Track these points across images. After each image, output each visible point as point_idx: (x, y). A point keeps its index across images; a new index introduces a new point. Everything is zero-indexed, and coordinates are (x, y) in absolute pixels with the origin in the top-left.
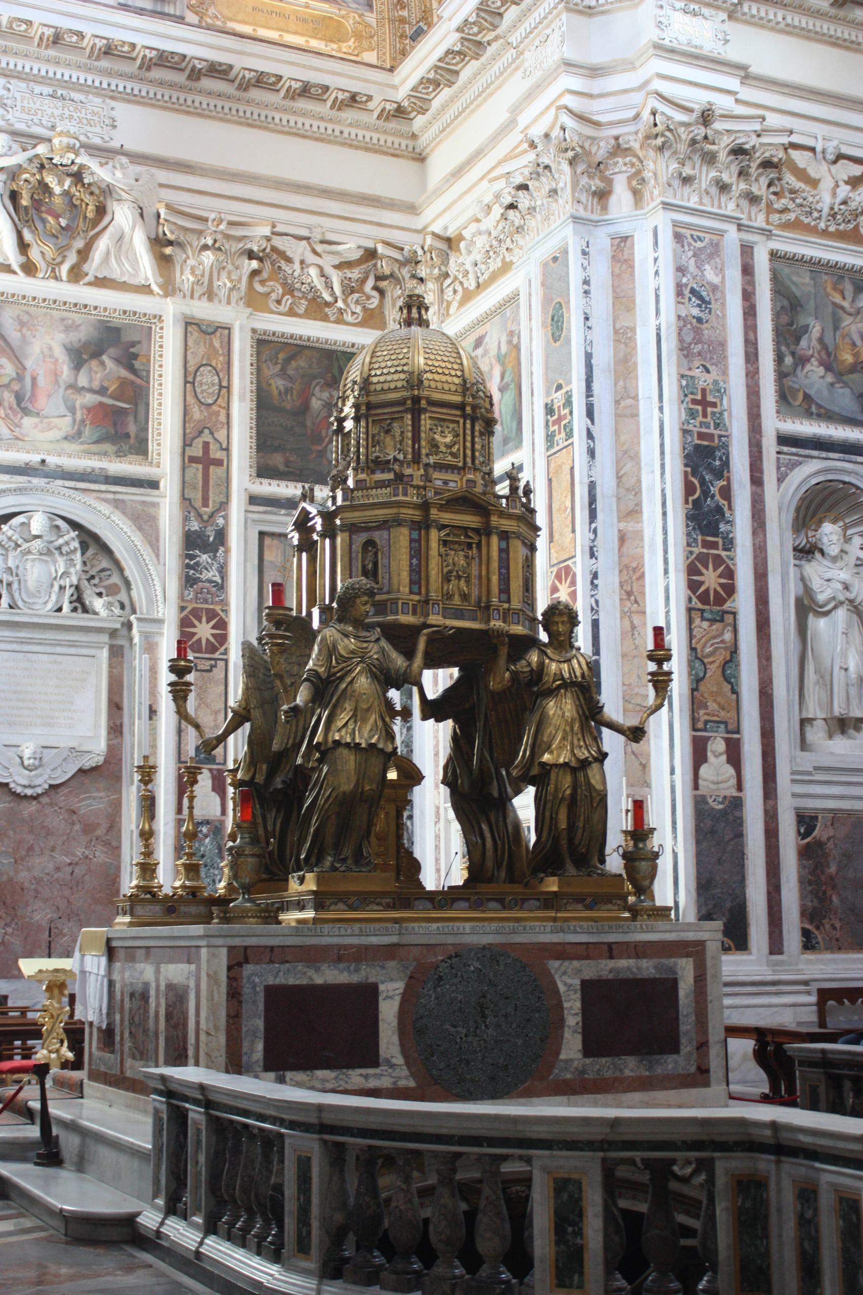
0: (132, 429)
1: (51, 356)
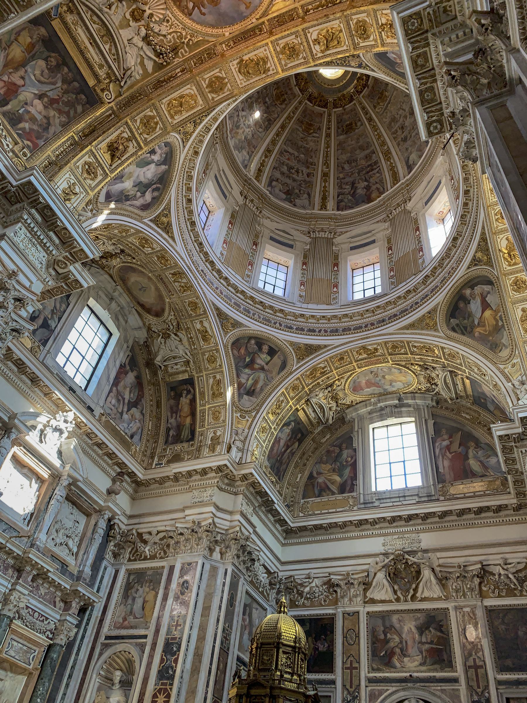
0: (445, 657)
1: (412, 631)
